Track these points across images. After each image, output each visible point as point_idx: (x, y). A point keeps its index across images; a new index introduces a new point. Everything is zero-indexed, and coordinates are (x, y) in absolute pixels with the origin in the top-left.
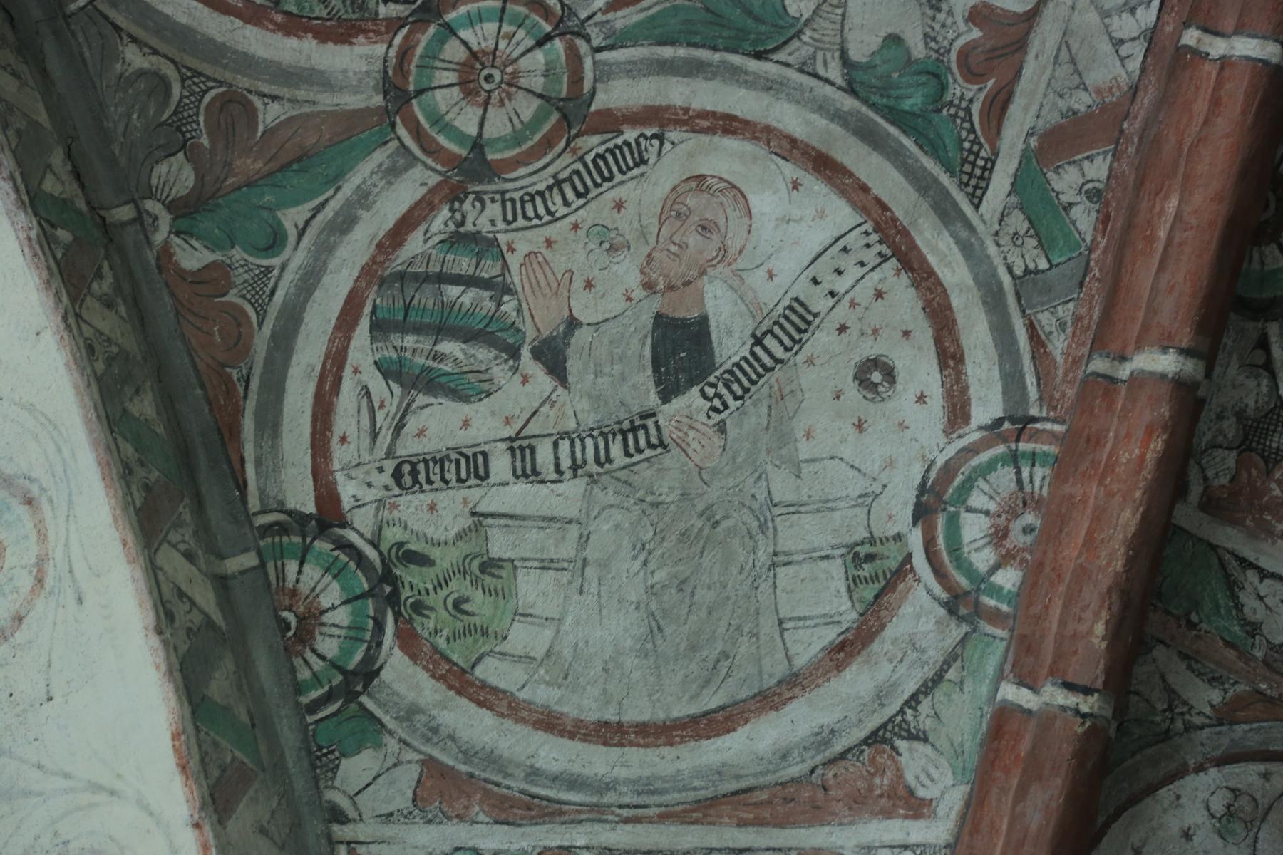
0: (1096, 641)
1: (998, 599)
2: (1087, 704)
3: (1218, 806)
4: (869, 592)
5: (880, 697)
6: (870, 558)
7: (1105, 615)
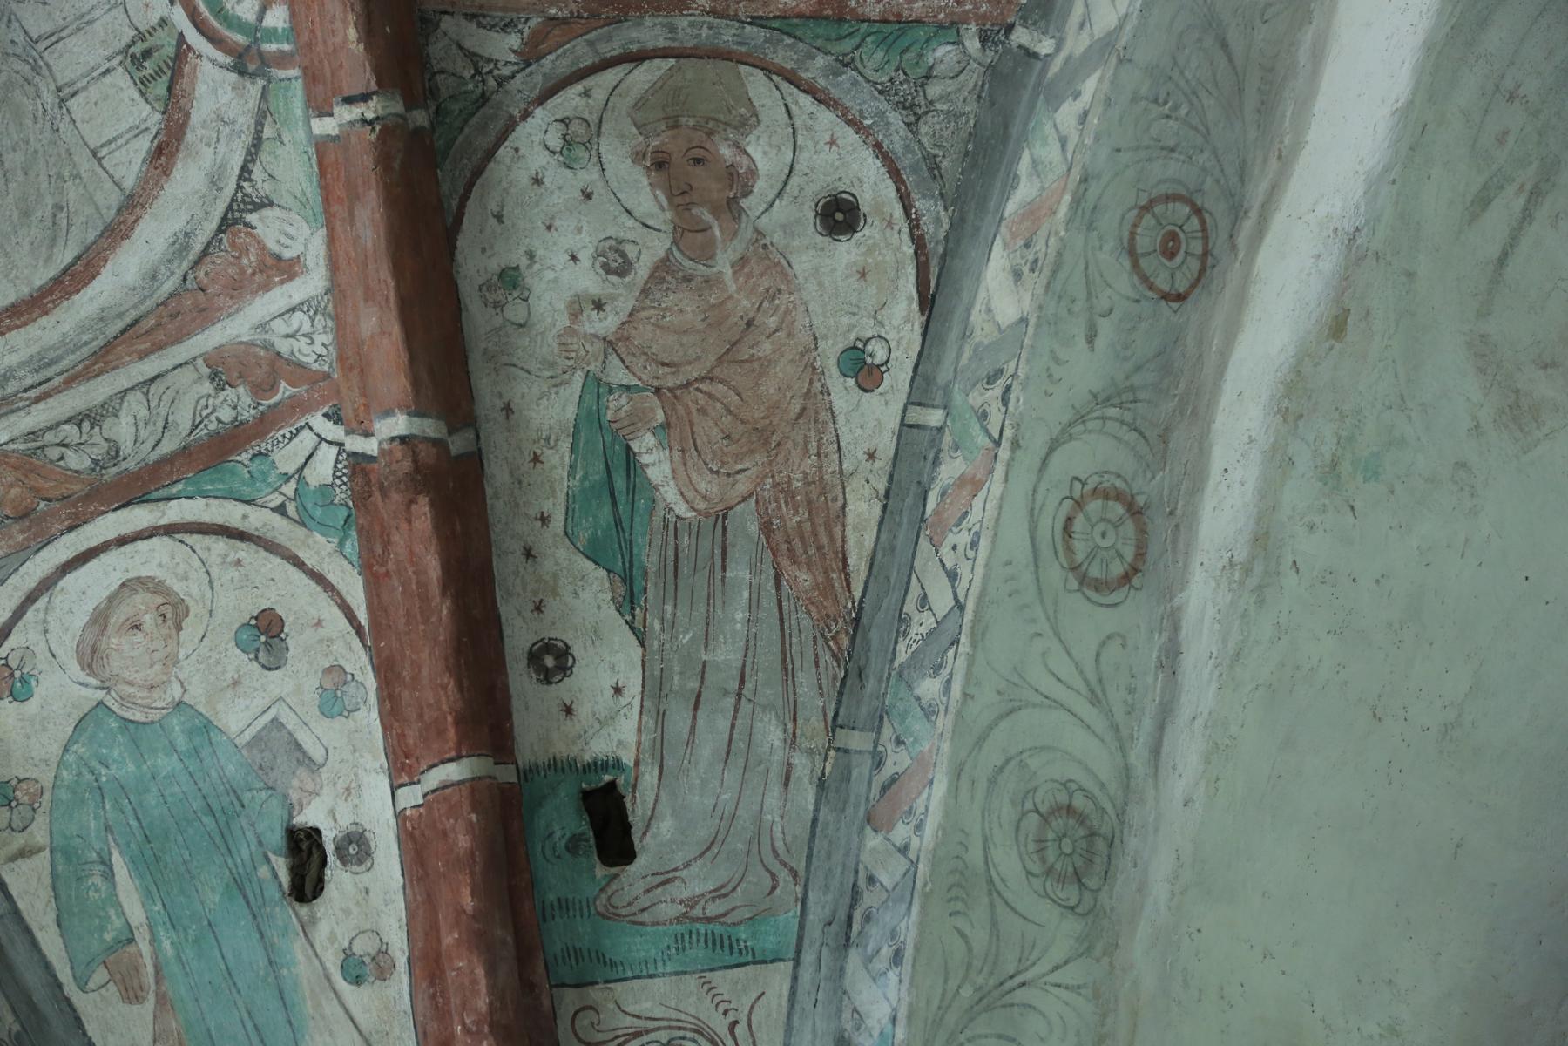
0: (353, 46)
1: (278, 42)
2: (370, 110)
3: (555, 141)
4: (160, 88)
5: (215, 182)
6: (147, 54)
7: (351, 18)
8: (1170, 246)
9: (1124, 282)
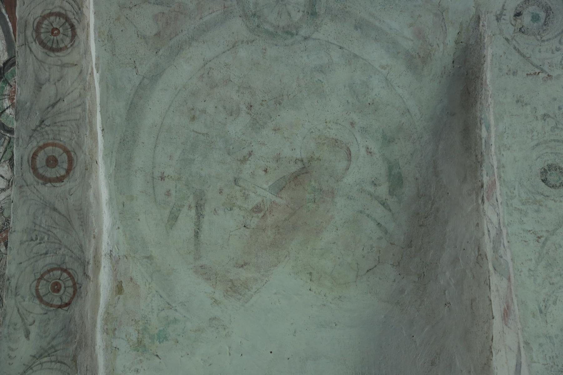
8: (56, 288)
9: (37, 309)
